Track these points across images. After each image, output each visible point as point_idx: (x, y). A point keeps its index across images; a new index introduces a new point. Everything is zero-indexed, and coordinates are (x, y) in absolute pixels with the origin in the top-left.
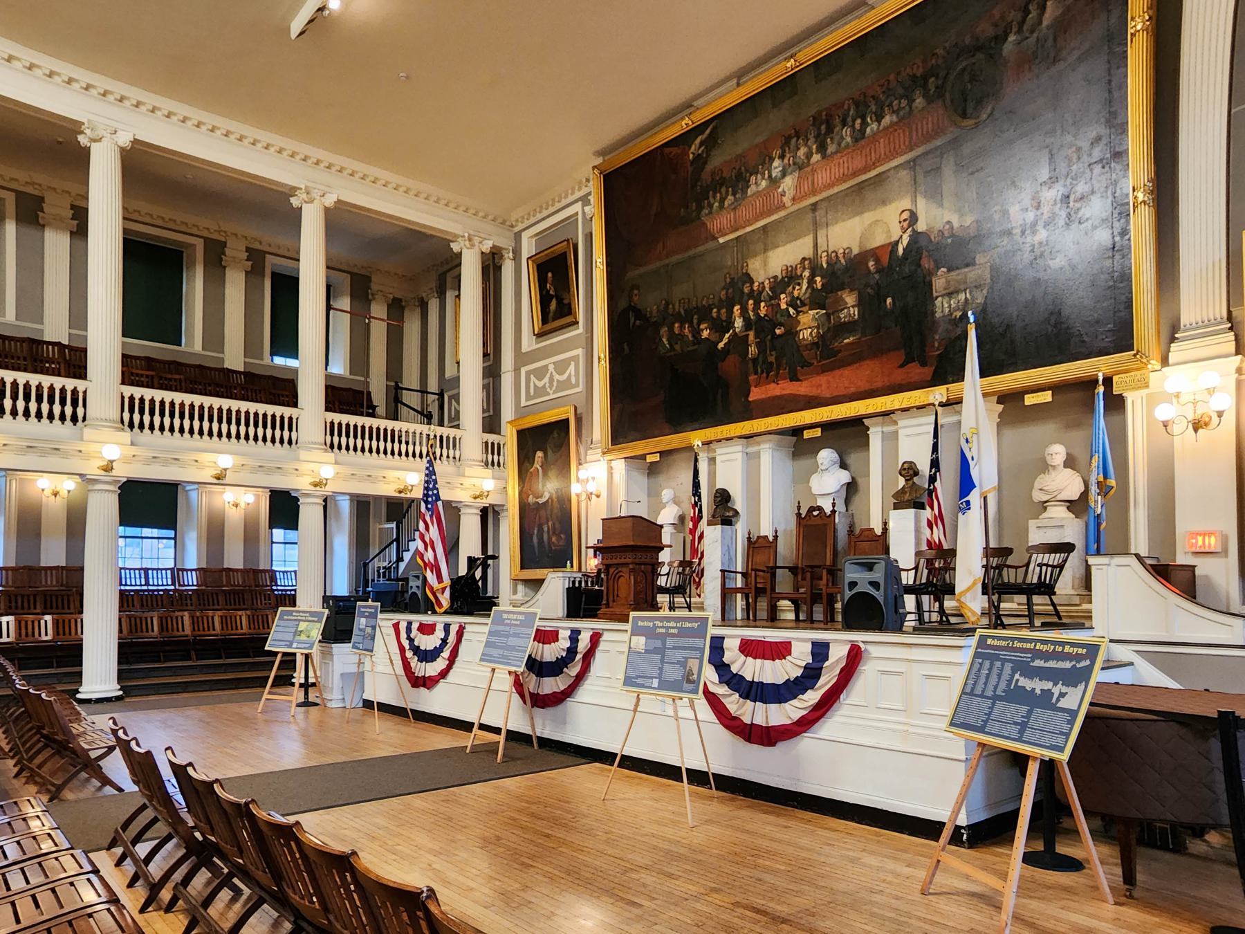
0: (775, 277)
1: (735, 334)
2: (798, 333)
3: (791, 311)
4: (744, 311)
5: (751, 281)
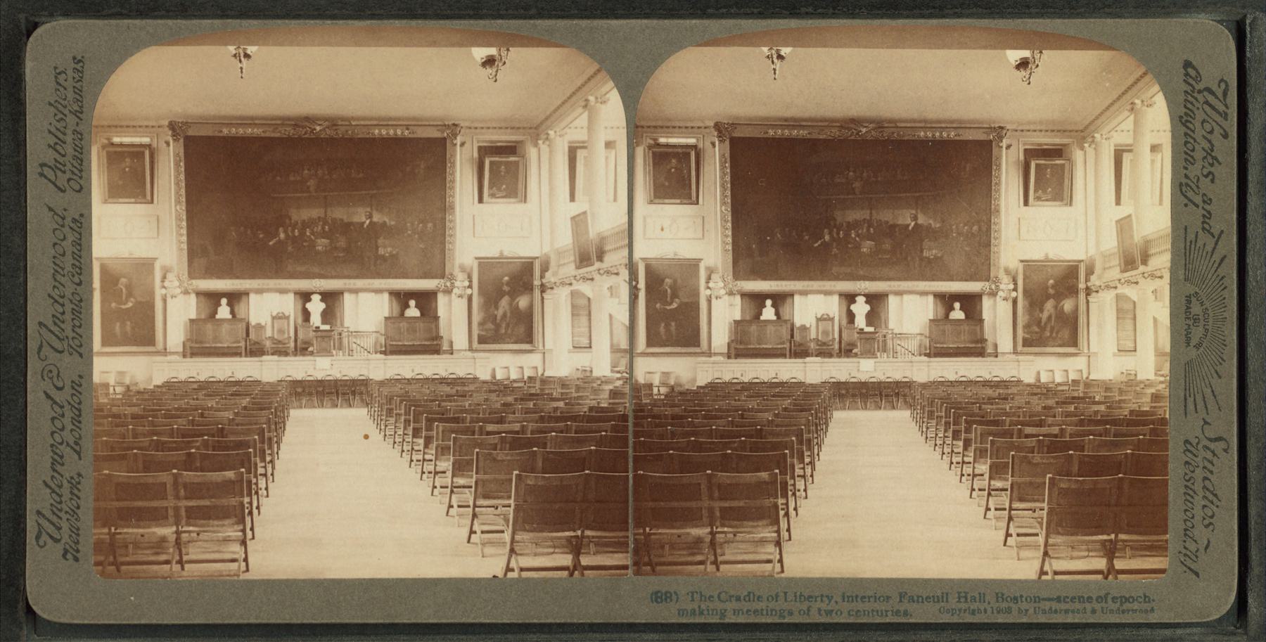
0: (304, 221)
1: (280, 241)
2: (315, 247)
3: (312, 237)
4: (285, 232)
5: (290, 219)
